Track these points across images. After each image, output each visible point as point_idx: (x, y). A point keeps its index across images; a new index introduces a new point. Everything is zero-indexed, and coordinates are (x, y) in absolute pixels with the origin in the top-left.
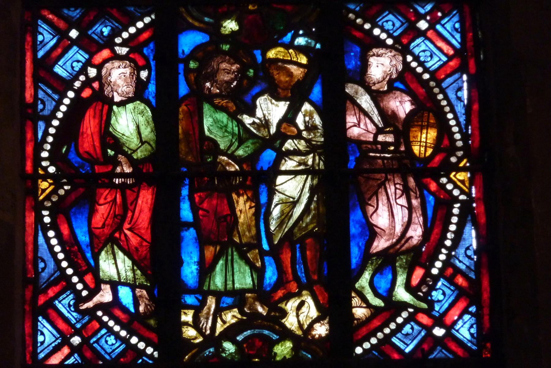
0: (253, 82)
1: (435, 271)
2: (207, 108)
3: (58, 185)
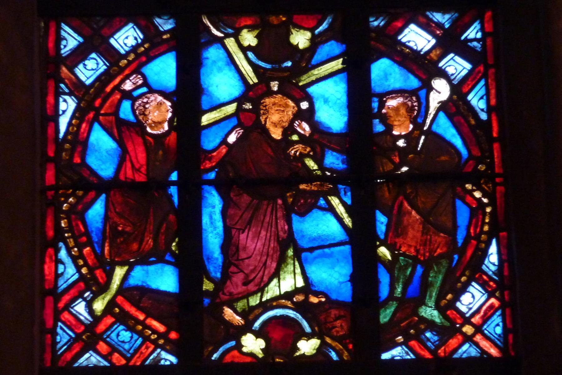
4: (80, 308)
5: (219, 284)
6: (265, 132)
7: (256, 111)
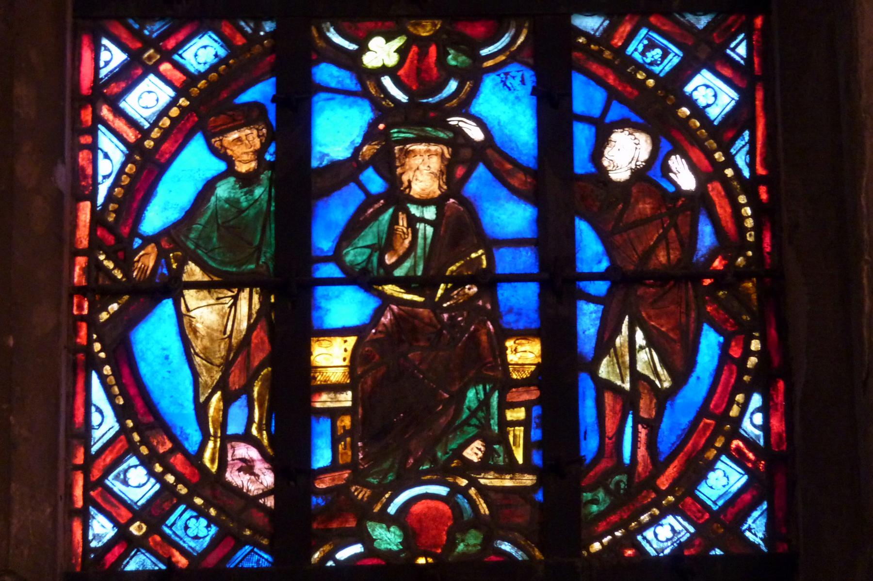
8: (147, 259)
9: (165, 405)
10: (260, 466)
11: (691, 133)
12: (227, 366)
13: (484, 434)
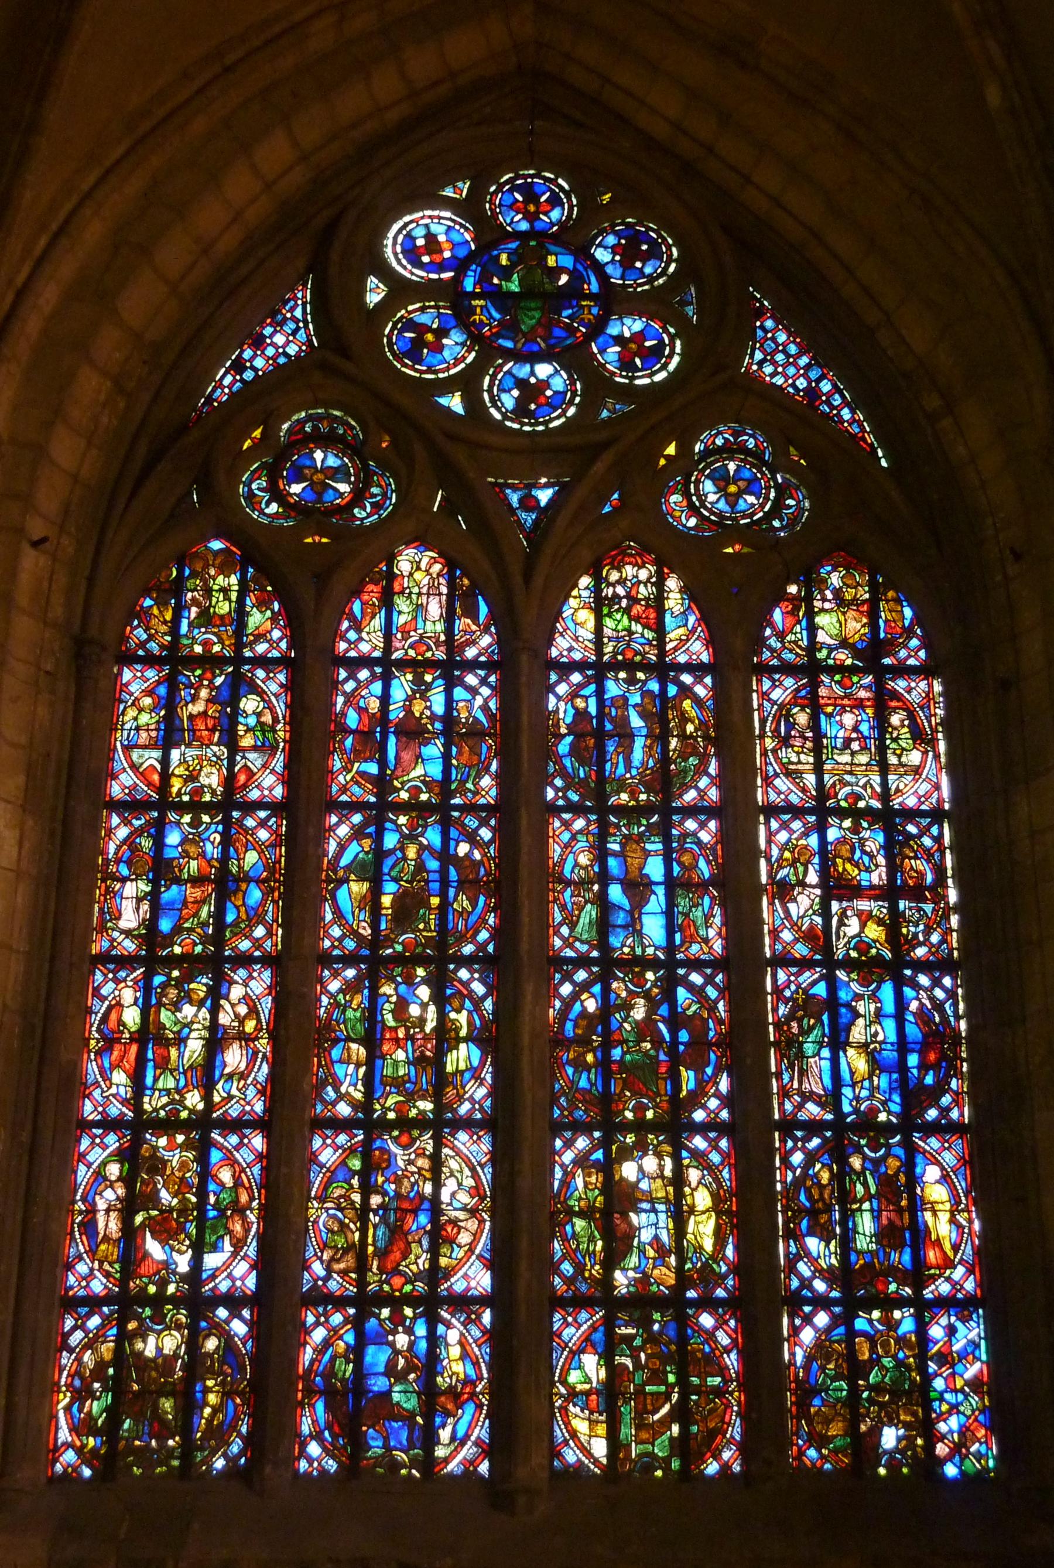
0: (183, 998)
1: (249, 1082)
2: (163, 1009)
3: (98, 1042)
4: (341, 778)
5: (393, 772)
6: (413, 713)
7: (410, 705)
8: (341, 873)
9: (343, 910)
10: (368, 928)
11: (480, 845)
12: (360, 902)
13: (425, 923)
